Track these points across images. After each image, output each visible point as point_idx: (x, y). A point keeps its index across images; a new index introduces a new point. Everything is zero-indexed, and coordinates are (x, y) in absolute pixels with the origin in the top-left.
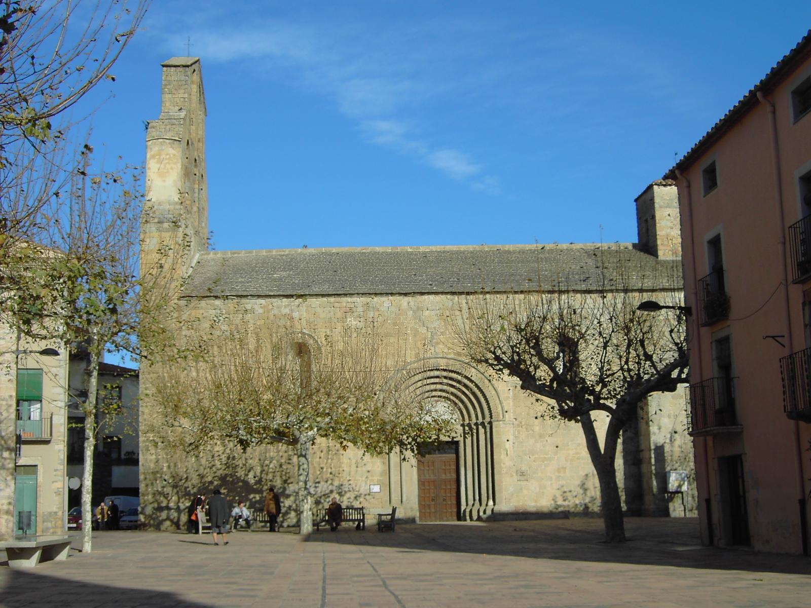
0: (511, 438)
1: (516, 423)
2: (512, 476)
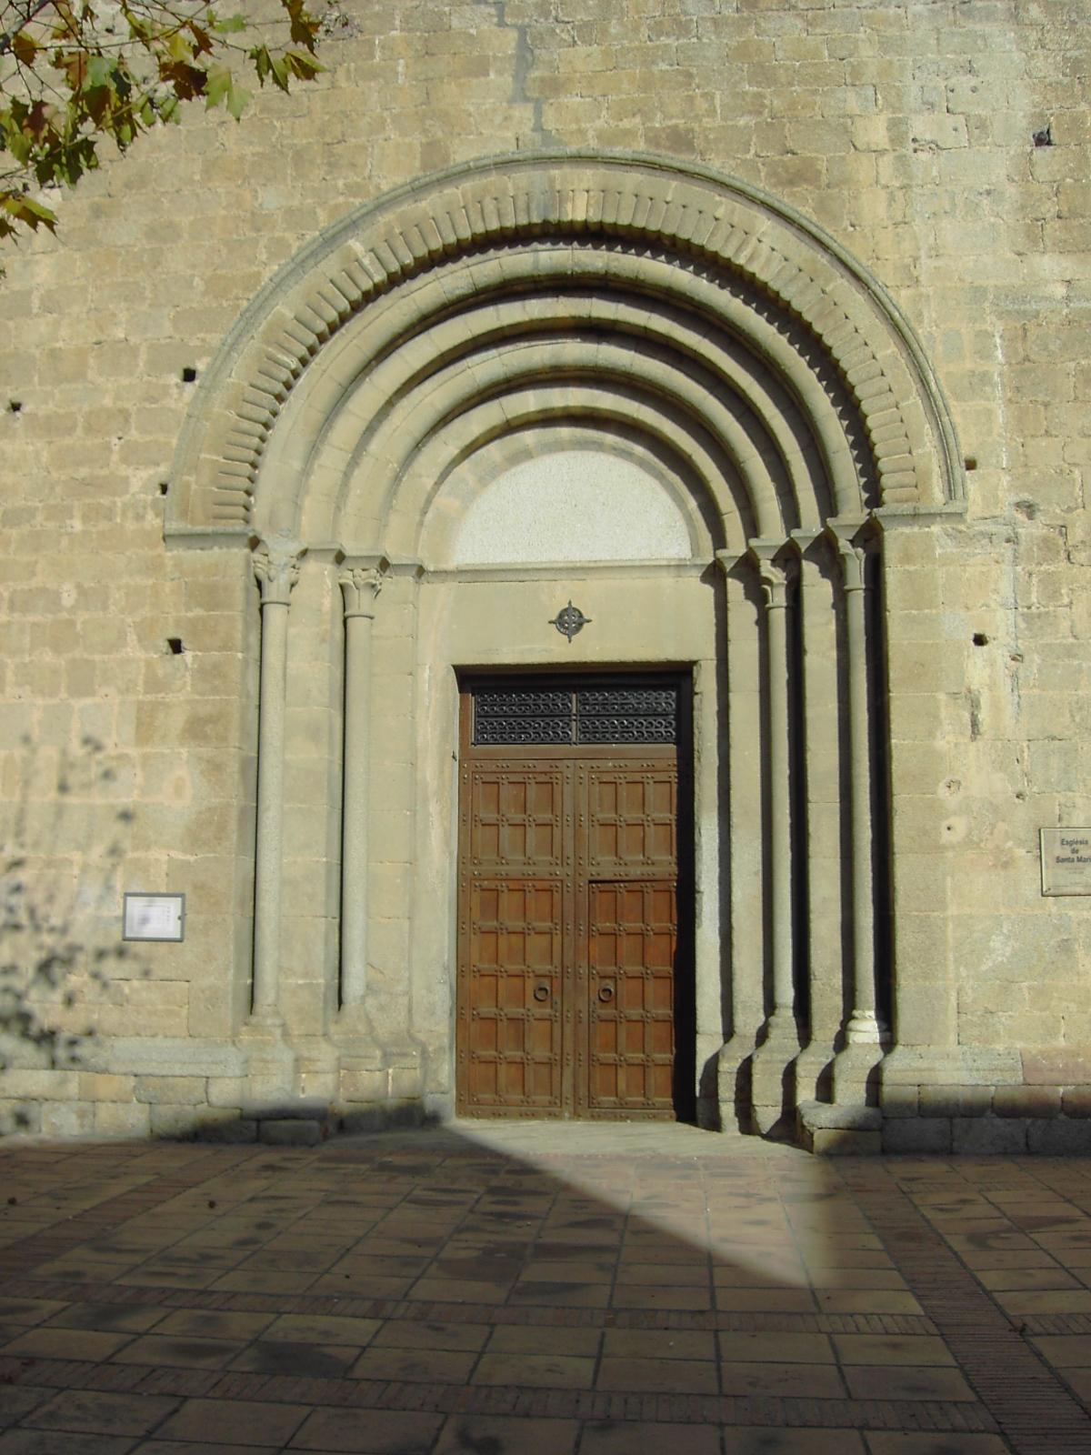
0: (1001, 625)
1: (1030, 530)
2: (1005, 863)
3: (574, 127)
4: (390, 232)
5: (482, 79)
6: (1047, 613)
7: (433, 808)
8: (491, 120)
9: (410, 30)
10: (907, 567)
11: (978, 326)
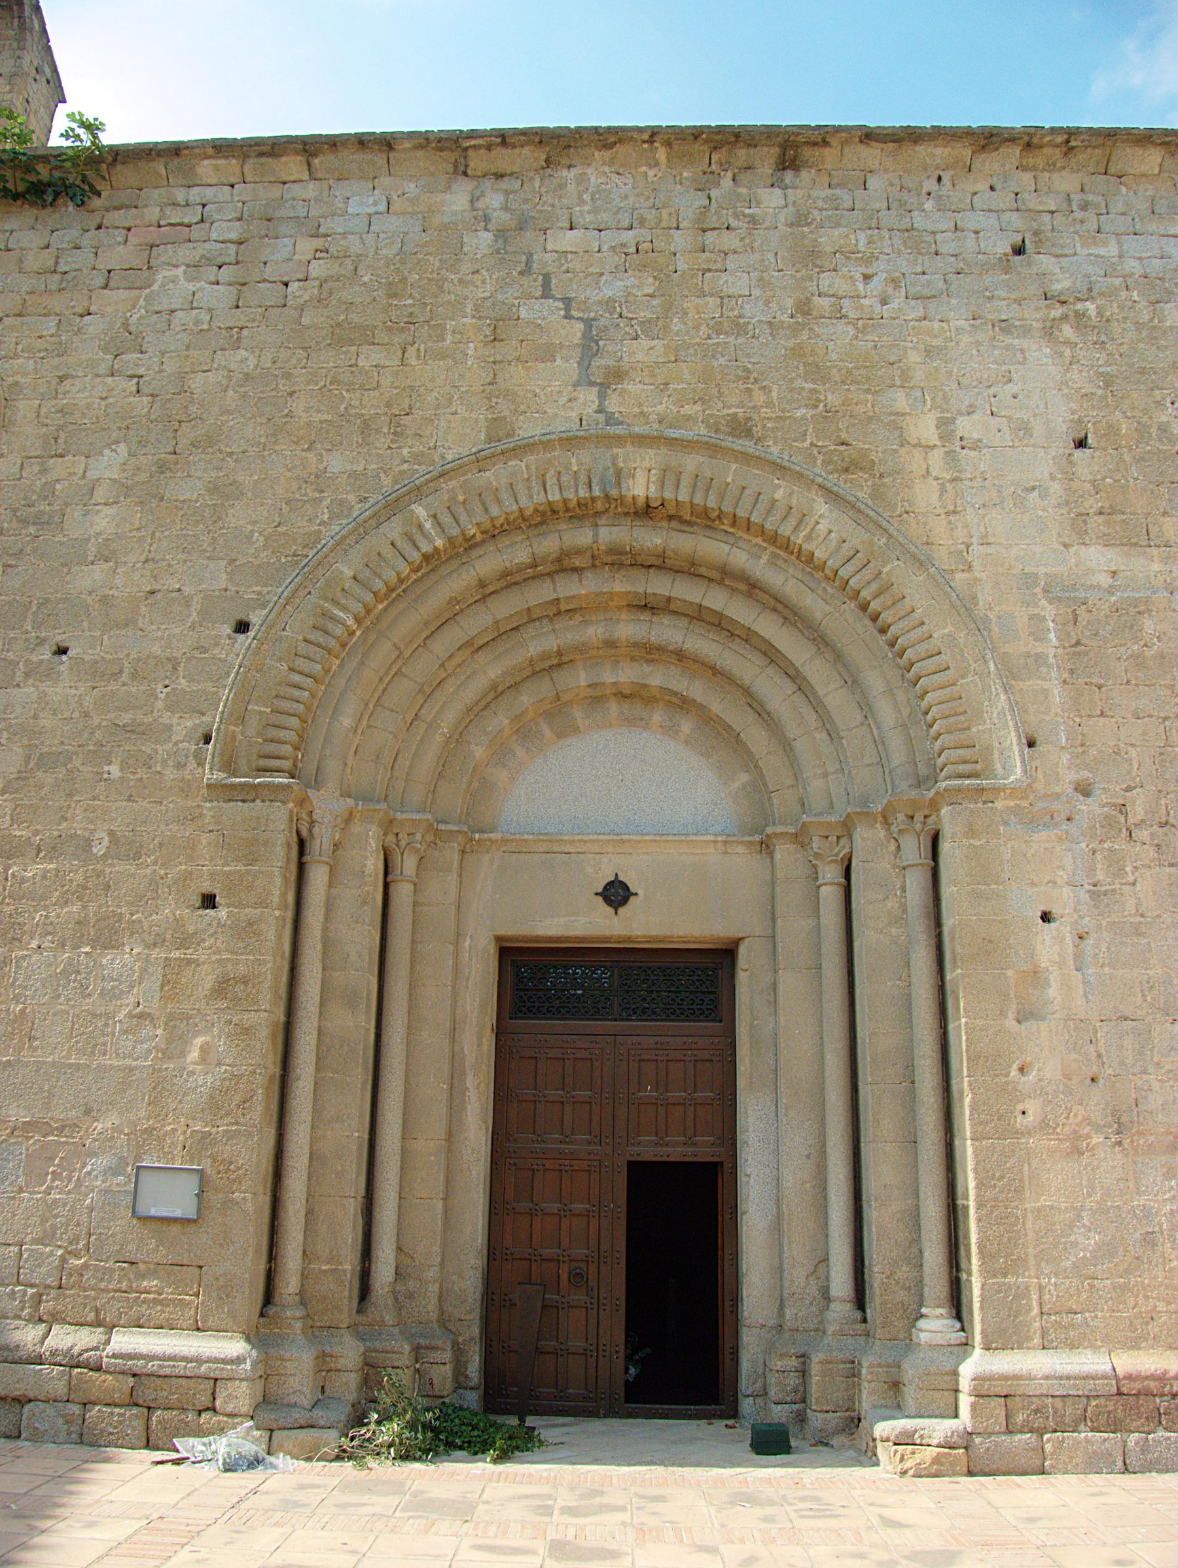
0: (1063, 901)
3: (637, 410)
4: (453, 499)
5: (548, 364)
6: (1113, 890)
7: (470, 1082)
8: (555, 398)
9: (480, 318)
10: (972, 841)
11: (1032, 610)
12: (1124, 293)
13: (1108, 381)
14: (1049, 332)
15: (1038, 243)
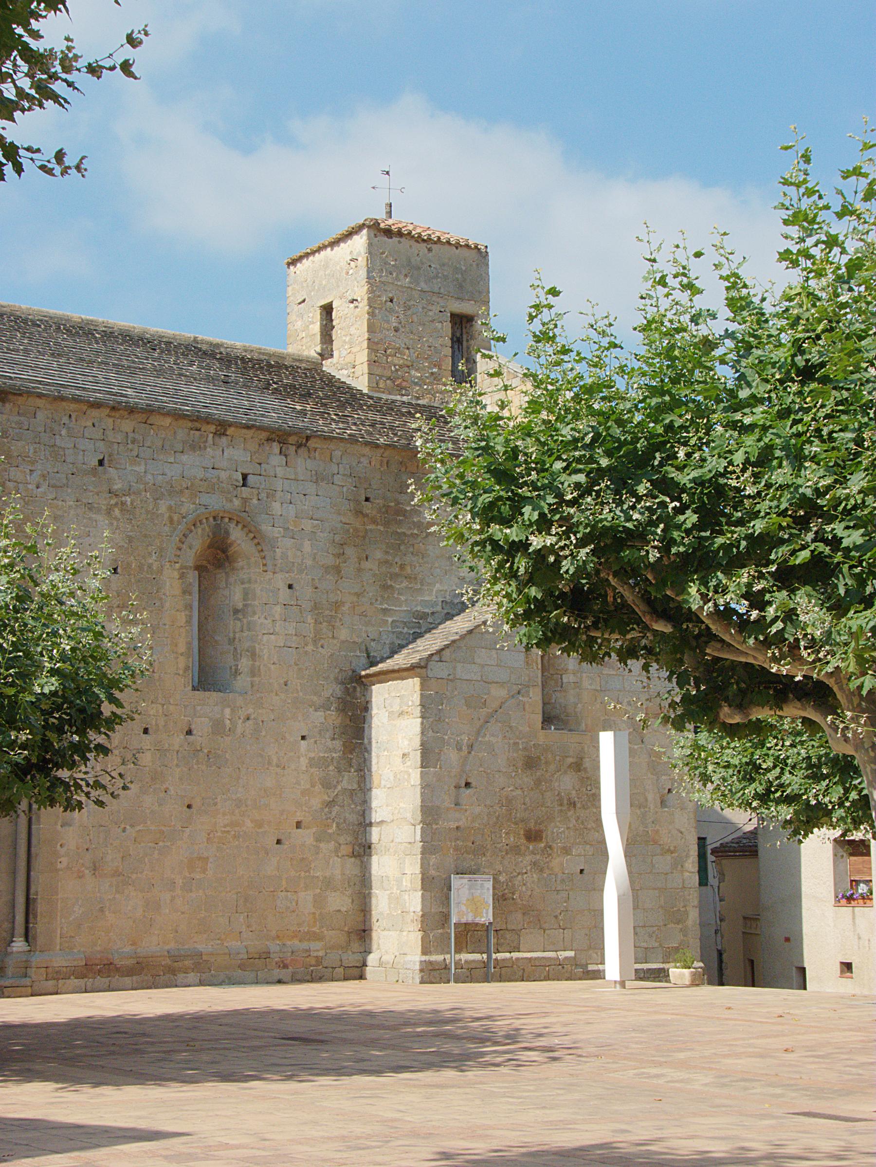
2: (81, 877)
12: (143, 493)
13: (130, 540)
14: (109, 512)
15: (110, 461)
